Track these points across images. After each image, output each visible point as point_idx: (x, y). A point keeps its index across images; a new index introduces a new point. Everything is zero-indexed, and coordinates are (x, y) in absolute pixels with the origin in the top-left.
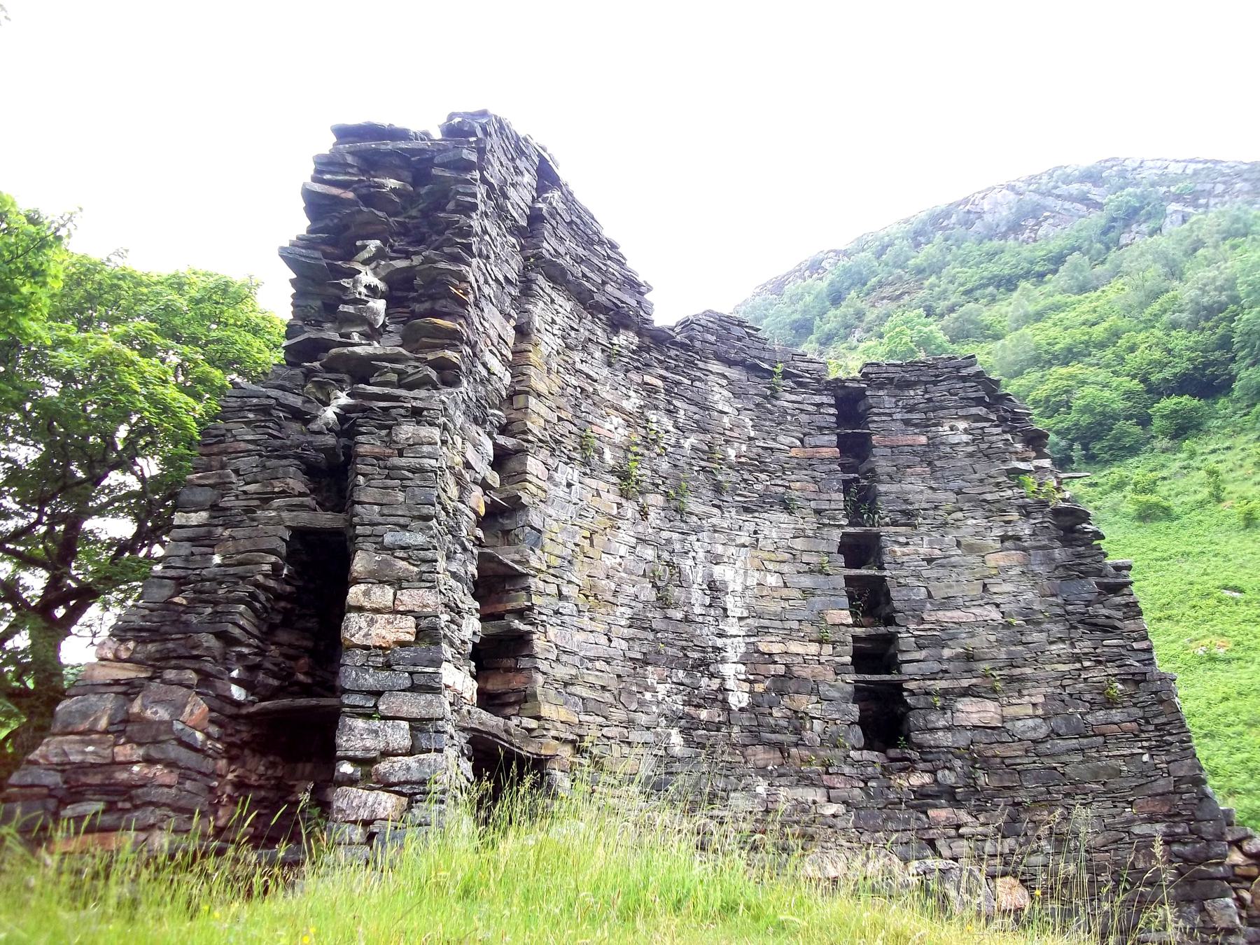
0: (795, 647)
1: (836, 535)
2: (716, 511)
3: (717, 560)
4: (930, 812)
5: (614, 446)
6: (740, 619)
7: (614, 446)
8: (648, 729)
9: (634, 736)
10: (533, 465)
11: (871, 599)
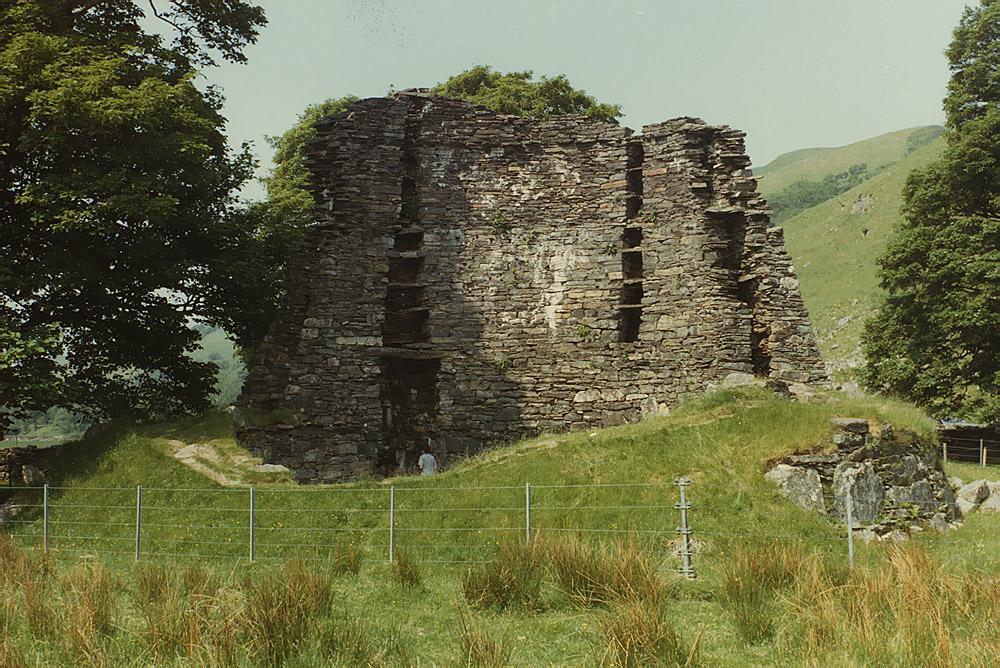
0: (589, 294)
1: (621, 231)
4: (641, 372)
5: (488, 211)
6: (563, 283)
10: (428, 237)
11: (634, 264)
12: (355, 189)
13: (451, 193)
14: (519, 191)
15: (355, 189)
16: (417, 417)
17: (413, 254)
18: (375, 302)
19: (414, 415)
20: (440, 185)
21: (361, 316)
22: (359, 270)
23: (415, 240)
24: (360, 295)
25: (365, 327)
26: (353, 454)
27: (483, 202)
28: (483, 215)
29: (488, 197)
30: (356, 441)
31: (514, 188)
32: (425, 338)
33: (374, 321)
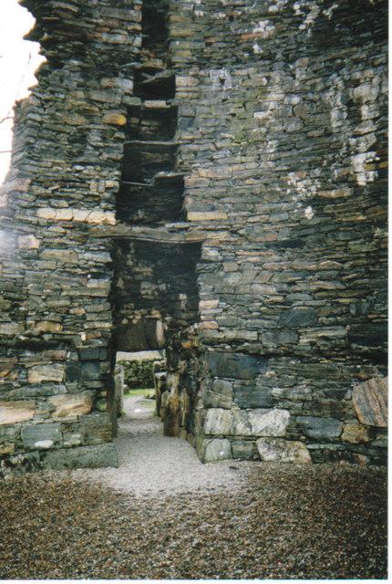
2: (355, 49)
3: (357, 83)
5: (261, 42)
7: (261, 42)
8: (288, 211)
9: (275, 218)
10: (181, 81)
12: (69, 7)
13: (210, 24)
14: (302, 9)
15: (69, 7)
16: (188, 329)
17: (162, 104)
18: (105, 165)
19: (186, 327)
20: (197, 13)
21: (83, 181)
22: (78, 120)
23: (167, 89)
24: (81, 153)
25: (87, 196)
26: (56, 383)
27: (255, 31)
28: (256, 47)
29: (262, 23)
30: (63, 361)
31: (296, 7)
32: (180, 215)
33: (102, 189)
